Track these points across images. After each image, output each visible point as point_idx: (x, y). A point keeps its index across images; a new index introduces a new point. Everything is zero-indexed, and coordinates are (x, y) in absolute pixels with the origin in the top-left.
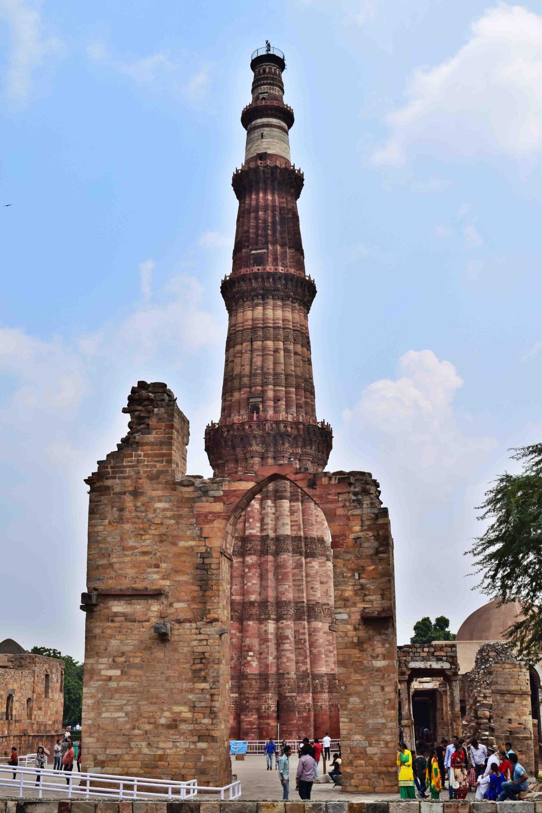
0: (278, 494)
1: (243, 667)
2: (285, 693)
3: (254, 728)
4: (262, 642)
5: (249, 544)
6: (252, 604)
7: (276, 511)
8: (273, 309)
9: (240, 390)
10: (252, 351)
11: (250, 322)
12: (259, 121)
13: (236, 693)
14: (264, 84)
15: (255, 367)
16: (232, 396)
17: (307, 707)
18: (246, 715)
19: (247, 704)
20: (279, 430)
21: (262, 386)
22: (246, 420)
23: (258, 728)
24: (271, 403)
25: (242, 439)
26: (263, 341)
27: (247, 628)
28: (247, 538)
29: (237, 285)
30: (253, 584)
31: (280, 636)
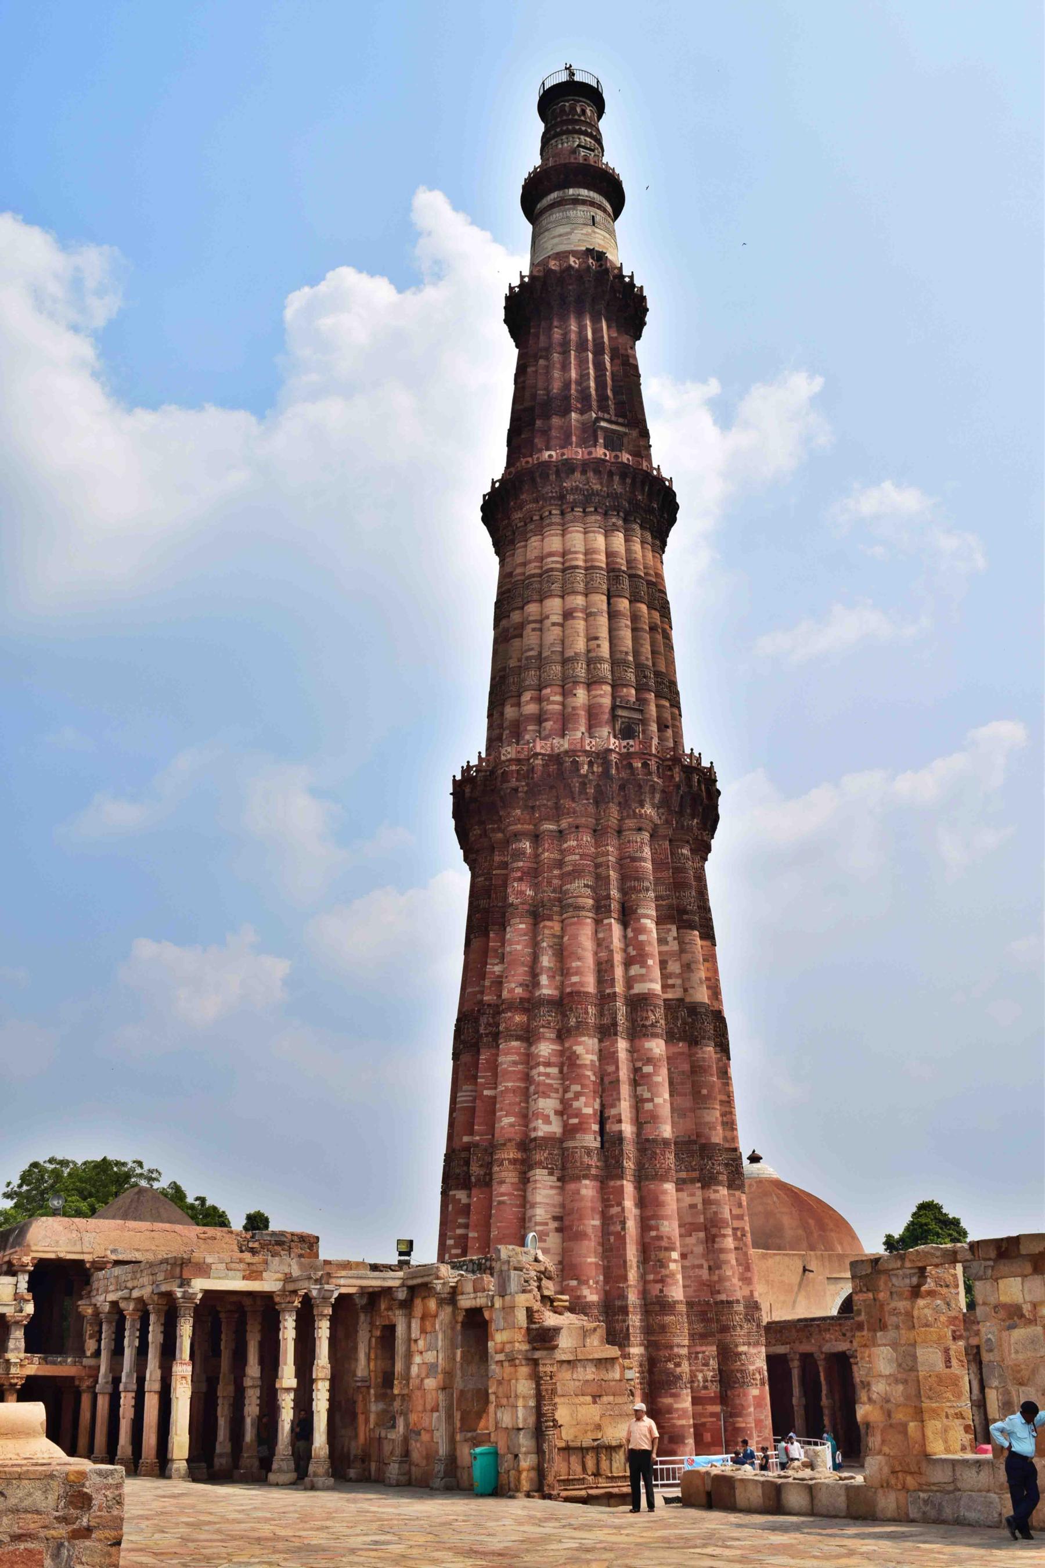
0: (685, 917)
1: (659, 1286)
2: (736, 1346)
3: (689, 1426)
4: (683, 1229)
5: (650, 1013)
6: (666, 1142)
7: (682, 951)
8: (642, 548)
9: (591, 684)
10: (613, 615)
11: (603, 557)
12: (584, 192)
13: (641, 1345)
14: (586, 134)
15: (625, 649)
16: (566, 693)
17: (757, 1376)
18: (673, 1395)
19: (678, 1370)
20: (690, 786)
21: (636, 690)
22: (632, 750)
23: (695, 1426)
24: (654, 727)
25: (622, 787)
26: (630, 602)
27: (662, 1198)
28: (646, 999)
29: (577, 475)
30: (665, 1100)
31: (712, 1221)
